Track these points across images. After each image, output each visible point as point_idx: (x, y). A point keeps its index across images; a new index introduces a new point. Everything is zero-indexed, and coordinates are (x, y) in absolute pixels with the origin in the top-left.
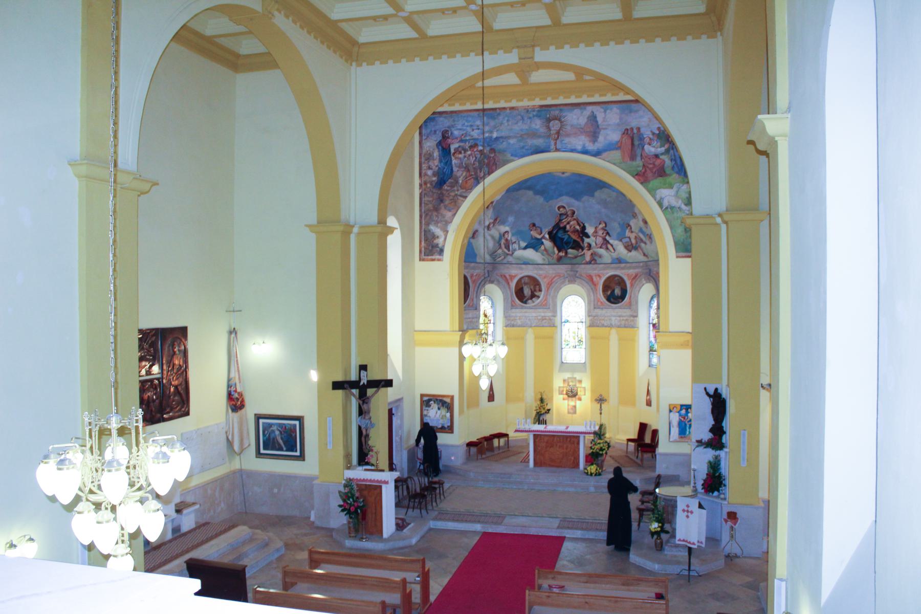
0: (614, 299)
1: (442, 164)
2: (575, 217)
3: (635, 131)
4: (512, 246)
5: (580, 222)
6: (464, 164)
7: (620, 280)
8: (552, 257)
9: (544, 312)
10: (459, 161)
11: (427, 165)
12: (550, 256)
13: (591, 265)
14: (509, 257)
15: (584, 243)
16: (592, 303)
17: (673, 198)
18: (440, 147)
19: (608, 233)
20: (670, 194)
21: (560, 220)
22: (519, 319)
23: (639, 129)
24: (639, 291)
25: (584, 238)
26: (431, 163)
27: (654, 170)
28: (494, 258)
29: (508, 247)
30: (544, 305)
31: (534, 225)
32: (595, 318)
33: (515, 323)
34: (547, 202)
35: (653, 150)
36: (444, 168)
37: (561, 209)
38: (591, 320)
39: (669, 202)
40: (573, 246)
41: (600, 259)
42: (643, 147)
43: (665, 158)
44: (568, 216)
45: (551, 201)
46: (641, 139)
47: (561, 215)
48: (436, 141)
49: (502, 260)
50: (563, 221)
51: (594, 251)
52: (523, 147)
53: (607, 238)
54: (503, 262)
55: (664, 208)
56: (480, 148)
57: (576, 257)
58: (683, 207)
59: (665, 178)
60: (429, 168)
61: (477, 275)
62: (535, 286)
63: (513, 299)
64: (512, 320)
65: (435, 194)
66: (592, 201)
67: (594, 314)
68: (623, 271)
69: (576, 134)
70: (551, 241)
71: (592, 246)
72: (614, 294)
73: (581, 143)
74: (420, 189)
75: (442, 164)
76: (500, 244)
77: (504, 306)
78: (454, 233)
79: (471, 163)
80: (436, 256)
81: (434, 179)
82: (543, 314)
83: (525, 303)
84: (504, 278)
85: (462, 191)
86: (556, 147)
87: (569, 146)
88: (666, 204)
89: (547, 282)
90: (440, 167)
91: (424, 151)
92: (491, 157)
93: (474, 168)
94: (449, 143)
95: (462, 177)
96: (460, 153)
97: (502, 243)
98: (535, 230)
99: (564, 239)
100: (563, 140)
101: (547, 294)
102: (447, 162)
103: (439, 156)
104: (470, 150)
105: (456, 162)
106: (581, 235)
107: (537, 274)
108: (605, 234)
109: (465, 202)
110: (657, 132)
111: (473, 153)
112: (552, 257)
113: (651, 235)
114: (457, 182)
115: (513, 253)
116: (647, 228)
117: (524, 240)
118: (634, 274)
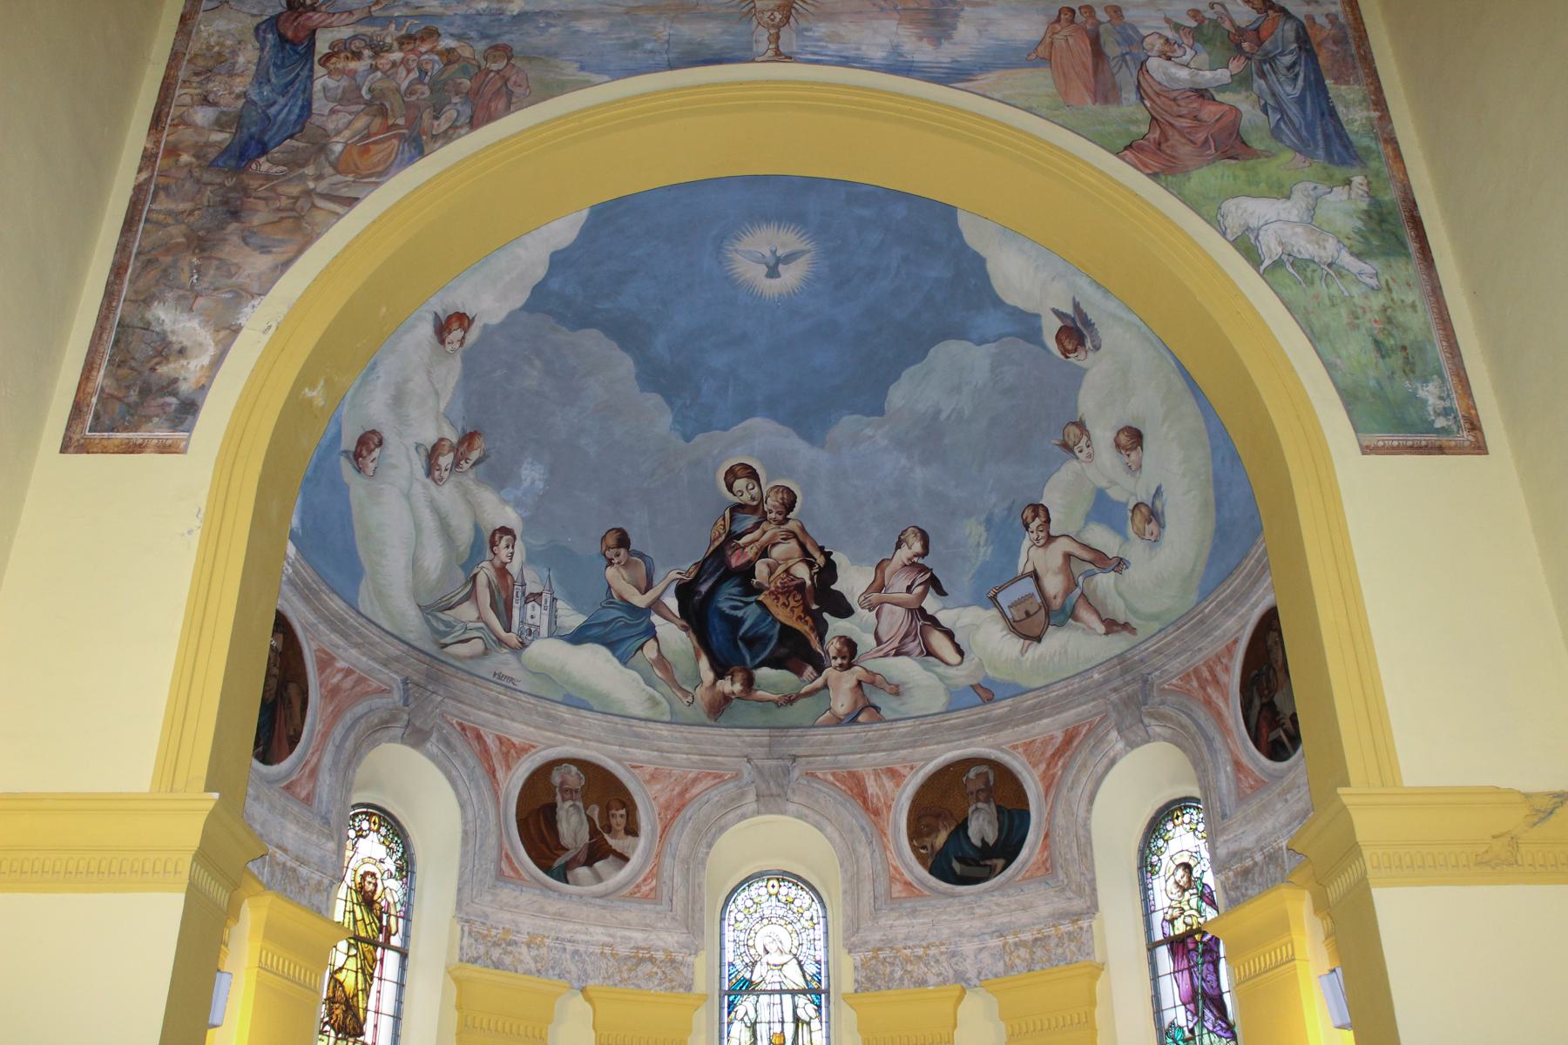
0: (961, 860)
1: (266, 91)
2: (792, 525)
3: (1102, 16)
4: (522, 608)
5: (814, 543)
6: (364, 91)
7: (991, 778)
8: (686, 693)
9: (647, 927)
10: (345, 82)
11: (198, 91)
12: (680, 689)
13: (857, 728)
14: (504, 655)
15: (828, 637)
16: (868, 886)
17: (1299, 230)
18: (270, 36)
19: (934, 584)
20: (1284, 216)
21: (732, 536)
22: (529, 946)
23: (1116, 11)
24: (1091, 801)
25: (826, 616)
26: (216, 87)
27: (1201, 136)
28: (435, 631)
29: (503, 612)
30: (646, 896)
31: (623, 540)
32: (882, 955)
33: (508, 960)
34: (688, 439)
35: (1183, 74)
36: (274, 103)
37: (740, 484)
38: (856, 968)
39: (1281, 243)
40: (783, 651)
41: (894, 702)
42: (1143, 63)
43: (1246, 105)
44: (764, 518)
45: (699, 438)
46: (1131, 39)
47: (737, 509)
48: (254, 16)
49: (471, 658)
50: (741, 542)
51: (875, 674)
52: (635, 45)
53: (931, 604)
54: (482, 673)
55: (1267, 262)
56: (446, 43)
57: (790, 700)
58: (1346, 259)
59: (1251, 163)
60: (205, 101)
61: (348, 672)
62: (608, 808)
63: (507, 846)
64: (496, 944)
65: (209, 188)
66: (875, 433)
67: (875, 937)
68: (1006, 736)
69: (860, 12)
70: (685, 629)
71: (859, 653)
72: (968, 838)
73: (882, 40)
74: (140, 170)
75: (266, 91)
76: (475, 575)
77: (463, 866)
78: (267, 338)
79: (398, 90)
80: (159, 428)
81: (217, 137)
82: (638, 936)
83: (562, 875)
84: (475, 744)
85: (339, 178)
86: (777, 48)
87: (833, 46)
88: (1270, 247)
89: (662, 800)
90: (255, 98)
91: (195, 46)
92: (492, 71)
93: (408, 106)
94: (311, 24)
95: (347, 133)
96: (357, 55)
97: (482, 580)
98: (626, 565)
99: (741, 621)
100: (810, 30)
101: (658, 855)
102: (292, 83)
103: (258, 64)
104: (401, 49)
105: (331, 83)
106: (815, 607)
107: (619, 761)
108: (918, 590)
109: (341, 222)
110: (1193, 24)
111: (412, 57)
112: (686, 693)
113: (1158, 492)
114: (322, 149)
115: (523, 645)
116: (1135, 469)
117: (576, 602)
118: (1059, 736)
